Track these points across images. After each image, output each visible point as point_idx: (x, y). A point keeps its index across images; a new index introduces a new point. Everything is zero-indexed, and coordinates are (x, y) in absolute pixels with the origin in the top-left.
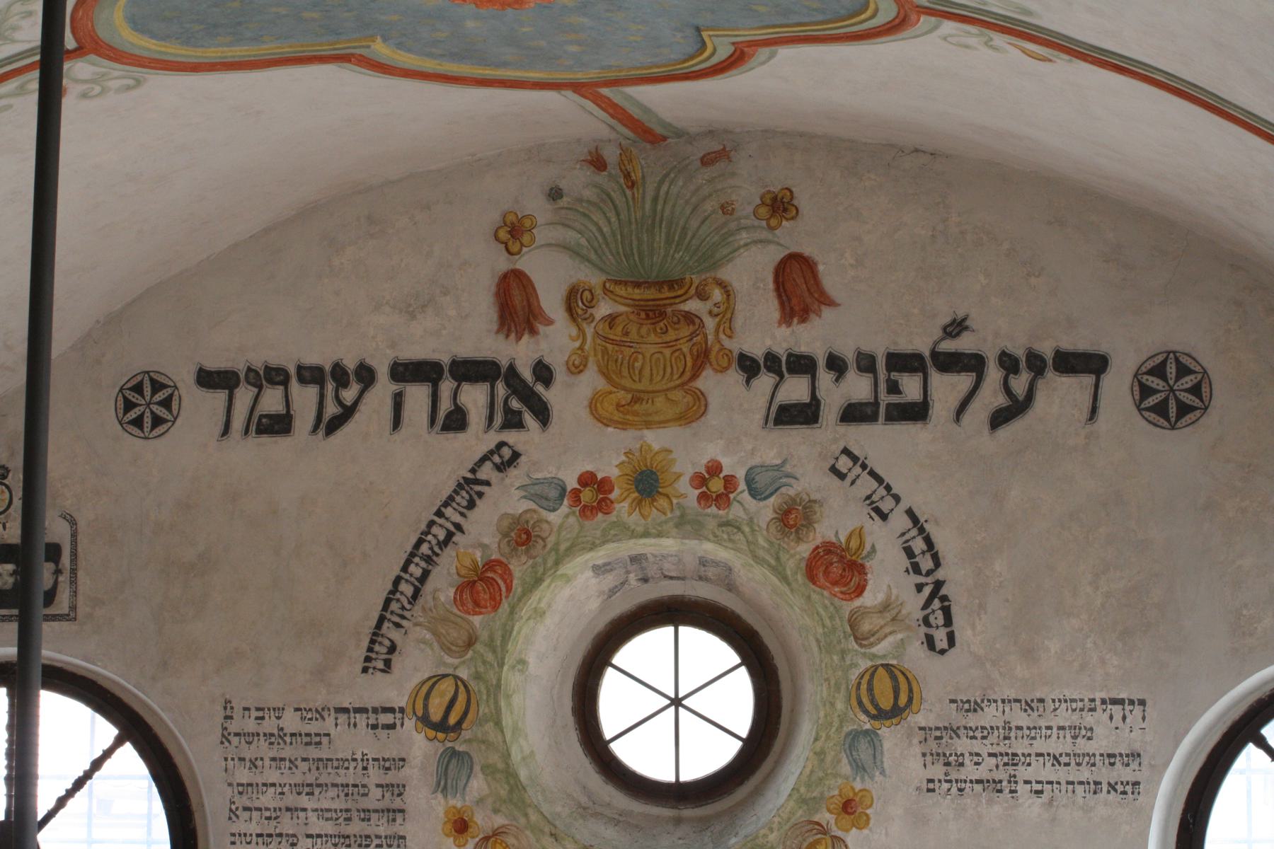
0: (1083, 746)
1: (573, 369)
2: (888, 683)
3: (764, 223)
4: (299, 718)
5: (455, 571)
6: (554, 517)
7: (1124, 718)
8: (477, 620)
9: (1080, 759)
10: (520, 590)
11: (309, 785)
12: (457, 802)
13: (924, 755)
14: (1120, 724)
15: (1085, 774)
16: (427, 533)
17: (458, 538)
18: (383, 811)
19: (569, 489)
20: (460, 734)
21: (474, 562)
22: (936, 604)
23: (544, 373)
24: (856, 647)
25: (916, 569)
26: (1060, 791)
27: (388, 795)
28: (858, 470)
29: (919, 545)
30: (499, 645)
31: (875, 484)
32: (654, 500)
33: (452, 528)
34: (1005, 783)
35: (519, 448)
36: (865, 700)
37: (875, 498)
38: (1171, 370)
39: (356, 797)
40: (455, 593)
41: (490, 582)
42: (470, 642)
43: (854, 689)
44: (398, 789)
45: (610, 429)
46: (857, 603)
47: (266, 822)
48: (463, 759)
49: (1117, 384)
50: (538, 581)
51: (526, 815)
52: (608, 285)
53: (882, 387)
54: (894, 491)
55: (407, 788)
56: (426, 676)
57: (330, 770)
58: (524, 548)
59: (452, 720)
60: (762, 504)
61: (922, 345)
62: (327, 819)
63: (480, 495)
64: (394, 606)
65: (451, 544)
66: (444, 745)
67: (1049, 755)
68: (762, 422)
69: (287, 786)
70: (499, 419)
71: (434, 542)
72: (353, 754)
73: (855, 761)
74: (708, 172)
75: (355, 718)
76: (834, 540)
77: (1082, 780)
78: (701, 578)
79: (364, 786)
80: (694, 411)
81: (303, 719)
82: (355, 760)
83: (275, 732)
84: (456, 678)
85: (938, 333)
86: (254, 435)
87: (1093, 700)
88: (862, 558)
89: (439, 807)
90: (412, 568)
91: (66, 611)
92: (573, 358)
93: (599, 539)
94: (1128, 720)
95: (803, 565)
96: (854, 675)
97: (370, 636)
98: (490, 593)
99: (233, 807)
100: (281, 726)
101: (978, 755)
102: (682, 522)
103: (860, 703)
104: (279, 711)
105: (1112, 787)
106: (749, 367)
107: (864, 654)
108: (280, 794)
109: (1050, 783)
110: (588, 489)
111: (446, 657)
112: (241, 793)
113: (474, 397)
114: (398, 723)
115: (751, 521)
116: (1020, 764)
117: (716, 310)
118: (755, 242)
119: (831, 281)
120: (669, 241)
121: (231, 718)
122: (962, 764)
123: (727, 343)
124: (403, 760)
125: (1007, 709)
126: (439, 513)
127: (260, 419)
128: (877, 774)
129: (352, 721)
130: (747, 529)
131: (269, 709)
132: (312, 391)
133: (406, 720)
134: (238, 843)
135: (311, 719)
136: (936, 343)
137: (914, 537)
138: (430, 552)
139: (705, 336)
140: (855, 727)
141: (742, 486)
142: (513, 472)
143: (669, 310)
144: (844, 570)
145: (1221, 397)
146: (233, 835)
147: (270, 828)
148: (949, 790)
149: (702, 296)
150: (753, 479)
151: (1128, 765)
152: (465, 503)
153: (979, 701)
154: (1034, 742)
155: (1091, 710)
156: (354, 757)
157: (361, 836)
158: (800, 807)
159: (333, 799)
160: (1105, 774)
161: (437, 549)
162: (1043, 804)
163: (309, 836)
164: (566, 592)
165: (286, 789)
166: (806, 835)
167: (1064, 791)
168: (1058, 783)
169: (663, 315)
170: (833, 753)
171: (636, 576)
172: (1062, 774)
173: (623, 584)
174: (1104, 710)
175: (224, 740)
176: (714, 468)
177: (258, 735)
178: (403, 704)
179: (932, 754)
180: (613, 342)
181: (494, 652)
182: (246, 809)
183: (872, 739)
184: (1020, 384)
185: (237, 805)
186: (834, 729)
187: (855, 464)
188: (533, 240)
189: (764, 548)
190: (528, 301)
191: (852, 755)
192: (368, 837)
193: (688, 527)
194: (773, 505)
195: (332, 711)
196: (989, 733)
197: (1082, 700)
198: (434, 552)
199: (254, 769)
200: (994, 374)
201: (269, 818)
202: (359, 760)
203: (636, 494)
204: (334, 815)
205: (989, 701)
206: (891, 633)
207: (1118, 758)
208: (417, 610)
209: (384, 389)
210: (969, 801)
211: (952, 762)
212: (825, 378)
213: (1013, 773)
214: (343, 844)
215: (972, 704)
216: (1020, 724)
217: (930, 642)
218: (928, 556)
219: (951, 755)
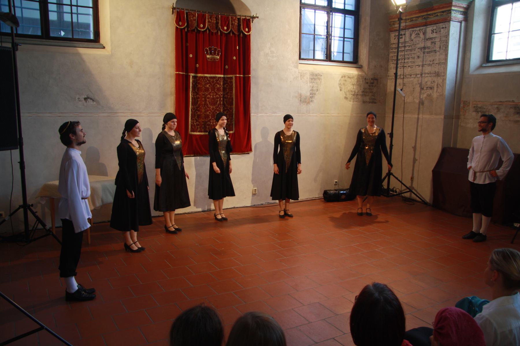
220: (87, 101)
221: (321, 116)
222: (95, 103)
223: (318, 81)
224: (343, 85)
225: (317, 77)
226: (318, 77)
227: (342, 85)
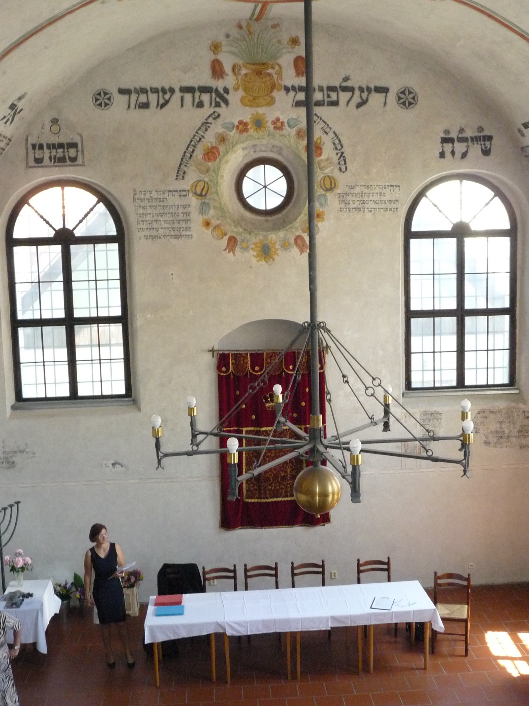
0: (383, 198)
2: (329, 180)
3: (290, 46)
6: (232, 134)
7: (394, 190)
9: (382, 202)
12: (206, 217)
14: (393, 192)
15: (383, 206)
17: (202, 140)
19: (235, 125)
21: (208, 147)
22: (342, 158)
23: (226, 90)
25: (336, 149)
27: (185, 215)
28: (319, 120)
29: (337, 142)
31: (324, 124)
32: (260, 129)
33: (201, 137)
34: (361, 209)
35: (220, 113)
36: (323, 186)
37: (324, 128)
38: (407, 92)
41: (213, 153)
42: (208, 171)
44: (188, 214)
45: (247, 108)
46: (320, 158)
49: (392, 96)
50: (227, 152)
53: (326, 96)
54: (330, 126)
56: (195, 180)
59: (204, 193)
62: (167, 223)
63: (209, 127)
64: (184, 160)
68: (291, 106)
70: (213, 104)
71: (196, 141)
74: (273, 30)
78: (271, 151)
79: (178, 213)
80: (271, 102)
81: (158, 194)
83: (150, 198)
84: (204, 181)
85: (341, 80)
87: (385, 185)
90: (189, 149)
99: (138, 221)
101: (354, 201)
102: (269, 135)
103: (321, 187)
104: (151, 192)
105: (391, 209)
106: (287, 89)
107: (322, 173)
109: (373, 208)
112: (140, 216)
113: (206, 98)
114: (187, 195)
115: (289, 135)
117: (277, 72)
118: (289, 52)
120: (262, 52)
121: (136, 194)
123: (280, 82)
126: (197, 132)
127: (139, 104)
130: (288, 137)
132: (155, 96)
136: (341, 83)
141: (286, 124)
142: (218, 120)
143: (263, 72)
145: (421, 100)
146: (139, 229)
147: (150, 226)
149: (273, 68)
152: (205, 129)
155: (385, 188)
160: (389, 206)
161: (196, 143)
164: (234, 156)
165: (154, 215)
169: (261, 74)
172: (377, 206)
173: (249, 153)
176: (278, 119)
180: (247, 81)
181: (215, 173)
182: (142, 221)
184: (364, 95)
187: (318, 118)
188: (221, 50)
192: (180, 228)
193: (271, 137)
198: (196, 144)
200: (357, 93)
203: (255, 127)
208: (191, 162)
209: (178, 95)
211: (347, 203)
217: (340, 169)
218: (339, 145)
220: (115, 467)
221: (442, 471)
222: (124, 468)
223: (435, 421)
224: (481, 424)
225: (434, 417)
226: (435, 416)
227: (479, 424)
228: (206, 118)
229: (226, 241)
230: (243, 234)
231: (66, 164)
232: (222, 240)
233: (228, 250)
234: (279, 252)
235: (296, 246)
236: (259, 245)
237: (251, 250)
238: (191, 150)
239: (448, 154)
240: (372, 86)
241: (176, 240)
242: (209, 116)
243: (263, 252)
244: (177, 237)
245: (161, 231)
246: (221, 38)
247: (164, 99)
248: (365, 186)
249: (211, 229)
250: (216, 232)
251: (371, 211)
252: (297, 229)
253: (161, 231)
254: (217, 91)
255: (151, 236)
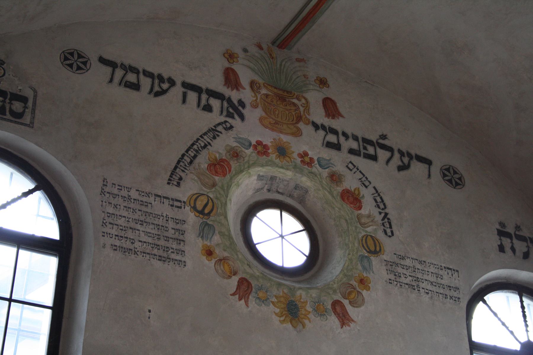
1: (253, 106)
3: (318, 85)
4: (138, 194)
5: (208, 158)
6: (246, 151)
7: (452, 275)
8: (217, 178)
10: (234, 172)
11: (142, 221)
13: (387, 270)
14: (451, 276)
15: (442, 291)
16: (197, 142)
17: (209, 147)
18: (175, 239)
19: (253, 144)
20: (209, 217)
21: (216, 157)
22: (386, 220)
23: (242, 103)
24: (360, 226)
25: (379, 207)
26: (434, 294)
28: (355, 170)
29: (379, 199)
30: (226, 190)
31: (362, 176)
33: (207, 143)
35: (233, 125)
36: (365, 245)
37: (363, 180)
38: (452, 171)
39: (163, 230)
40: (208, 166)
41: (222, 166)
42: (214, 185)
43: (361, 241)
44: (183, 233)
45: (267, 130)
46: (359, 212)
47: (120, 231)
48: (210, 227)
49: (436, 170)
50: (242, 171)
51: (237, 255)
52: (265, 84)
53: (361, 147)
55: (186, 232)
56: (195, 192)
57: (151, 217)
58: (236, 158)
59: (206, 211)
60: (323, 170)
61: (374, 138)
62: (149, 236)
64: (181, 164)
65: (206, 148)
66: (202, 220)
67: (429, 281)
68: (321, 145)
69: (131, 219)
70: (225, 113)
72: (162, 214)
73: (363, 265)
74: (297, 64)
75: (164, 200)
76: (349, 189)
77: (441, 292)
79: (166, 227)
82: (163, 216)
83: (127, 196)
84: (208, 196)
85: (378, 137)
86: (123, 86)
88: (360, 198)
89: (200, 243)
90: (190, 152)
91: (28, 123)
92: (253, 103)
93: (264, 164)
94: (454, 276)
95: (340, 194)
96: (360, 236)
97: (171, 172)
98: (222, 170)
99: (105, 221)
100: (129, 195)
102: (295, 167)
103: (363, 246)
104: (129, 189)
106: (316, 127)
107: (363, 230)
108: (127, 221)
109: (431, 291)
110: (260, 146)
111: (204, 188)
113: (215, 103)
114: (183, 207)
115: (320, 174)
116: (420, 282)
119: (342, 108)
121: (106, 186)
122: (400, 277)
123: (307, 116)
124: (185, 221)
125: (414, 262)
126: (201, 136)
128: (371, 272)
129: (162, 201)
130: (319, 177)
131: (124, 187)
132: (149, 81)
133: (186, 207)
134: (106, 236)
135: (144, 196)
136: (377, 140)
137: (377, 196)
138: (197, 149)
139: (300, 112)
140: (362, 254)
141: (316, 162)
144: (354, 200)
146: (104, 233)
147: (122, 234)
148: (397, 284)
150: (320, 161)
151: (455, 291)
152: (212, 137)
153: (404, 257)
154: (423, 275)
155: (442, 269)
156: (162, 215)
157: (164, 247)
158: (345, 277)
159: (152, 229)
160: (448, 292)
161: (200, 149)
162: (429, 298)
163: (140, 241)
165: (130, 220)
166: (348, 288)
167: (435, 295)
168: (433, 291)
170: (355, 261)
171: (268, 187)
173: (262, 189)
174: (446, 271)
175: (102, 193)
177: (118, 195)
178: (185, 200)
179: (390, 270)
180: (267, 102)
181: (224, 190)
182: (110, 223)
183: (368, 260)
185: (106, 221)
186: (355, 253)
188: (238, 61)
189: (325, 185)
190: (236, 79)
191: (362, 264)
192: (167, 248)
194: (327, 172)
195: (153, 195)
196: (408, 268)
197: (438, 265)
199: (115, 208)
201: (122, 230)
202: (165, 217)
204: (152, 236)
205: (407, 257)
206: (372, 225)
207: (452, 288)
208: (191, 168)
210: (404, 290)
212: (342, 139)
213: (418, 284)
214: (156, 248)
215: (402, 257)
216: (419, 268)
219: (396, 272)
228: (214, 125)
229: (236, 283)
230: (261, 280)
231: (5, 117)
232: (229, 281)
233: (237, 296)
234: (311, 316)
235: (335, 314)
236: (282, 299)
237: (271, 304)
238: (193, 155)
239: (508, 248)
240: (413, 152)
241: (160, 263)
242: (219, 124)
243: (289, 311)
244: (164, 259)
245: (137, 244)
246: (238, 50)
247: (160, 87)
248: (416, 259)
249: (213, 261)
250: (222, 267)
251: (428, 293)
252: (335, 291)
253: (137, 244)
254: (229, 100)
255: (122, 248)
